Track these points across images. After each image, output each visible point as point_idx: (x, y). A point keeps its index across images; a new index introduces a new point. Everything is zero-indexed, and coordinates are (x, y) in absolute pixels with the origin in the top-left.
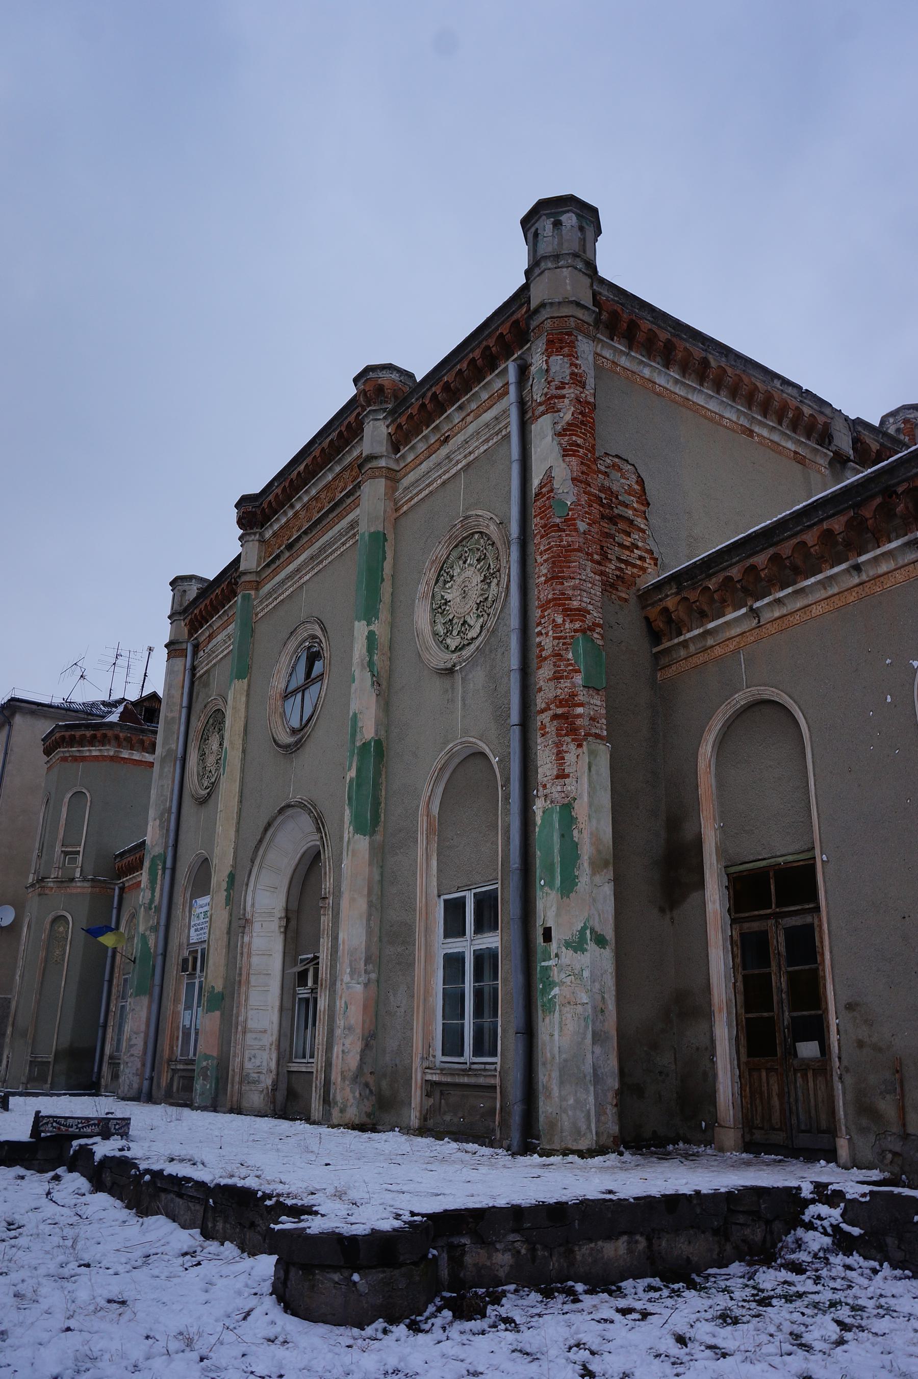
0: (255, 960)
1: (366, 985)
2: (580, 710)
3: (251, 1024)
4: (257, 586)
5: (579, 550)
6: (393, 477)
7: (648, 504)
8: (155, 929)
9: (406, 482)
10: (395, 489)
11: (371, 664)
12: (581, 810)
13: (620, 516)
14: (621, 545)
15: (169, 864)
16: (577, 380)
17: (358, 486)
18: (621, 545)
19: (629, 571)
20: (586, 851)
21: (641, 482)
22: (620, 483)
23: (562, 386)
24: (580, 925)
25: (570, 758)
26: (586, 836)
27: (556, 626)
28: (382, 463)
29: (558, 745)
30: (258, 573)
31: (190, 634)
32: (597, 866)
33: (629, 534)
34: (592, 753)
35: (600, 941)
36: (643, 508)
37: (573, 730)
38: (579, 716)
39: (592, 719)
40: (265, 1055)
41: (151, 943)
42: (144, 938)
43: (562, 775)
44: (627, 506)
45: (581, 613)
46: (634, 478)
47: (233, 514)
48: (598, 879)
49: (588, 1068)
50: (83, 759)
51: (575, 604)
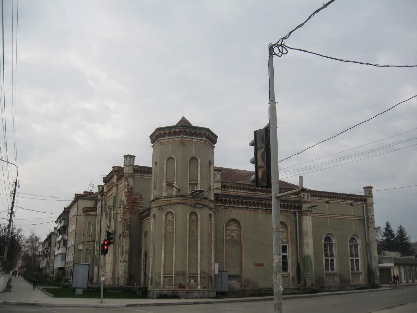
0: (107, 261)
1: (113, 266)
2: (125, 233)
3: (106, 271)
4: (107, 195)
5: (126, 211)
6: (117, 186)
7: (142, 199)
8: (97, 254)
9: (119, 187)
10: (118, 188)
11: (114, 218)
12: (124, 246)
13: (137, 202)
14: (137, 207)
15: (99, 242)
16: (128, 185)
17: (113, 187)
18: (137, 207)
19: (138, 210)
20: (124, 251)
21: (141, 195)
22: (137, 197)
23: (126, 186)
24: (123, 260)
25: (123, 239)
26: (125, 249)
27: (123, 222)
28: (116, 184)
29: (122, 238)
30: (106, 192)
31: (101, 197)
32: (126, 253)
33: (138, 204)
34: (126, 239)
35: (126, 262)
36: (141, 199)
37: (124, 236)
38: (125, 234)
39: (127, 234)
40: (108, 276)
41: (97, 257)
42: (96, 257)
43: (123, 242)
44: (138, 200)
45: (126, 220)
46: (140, 195)
47: (103, 180)
48: (126, 254)
49: (123, 276)
50: (90, 215)
51: (125, 219)
